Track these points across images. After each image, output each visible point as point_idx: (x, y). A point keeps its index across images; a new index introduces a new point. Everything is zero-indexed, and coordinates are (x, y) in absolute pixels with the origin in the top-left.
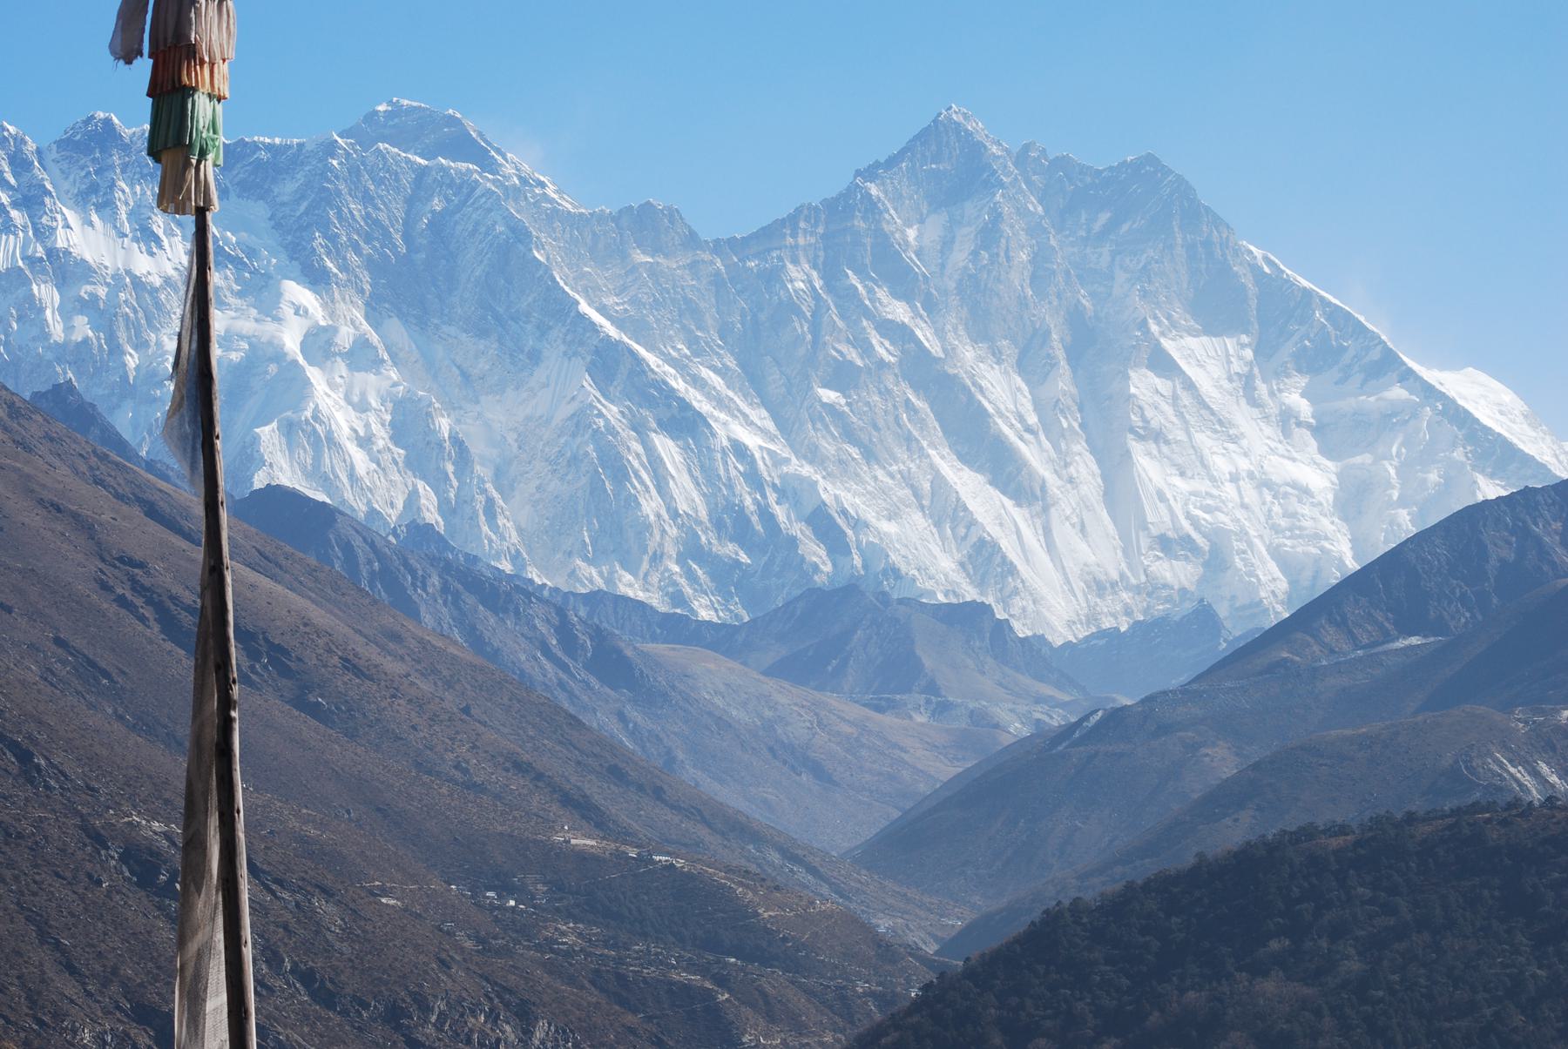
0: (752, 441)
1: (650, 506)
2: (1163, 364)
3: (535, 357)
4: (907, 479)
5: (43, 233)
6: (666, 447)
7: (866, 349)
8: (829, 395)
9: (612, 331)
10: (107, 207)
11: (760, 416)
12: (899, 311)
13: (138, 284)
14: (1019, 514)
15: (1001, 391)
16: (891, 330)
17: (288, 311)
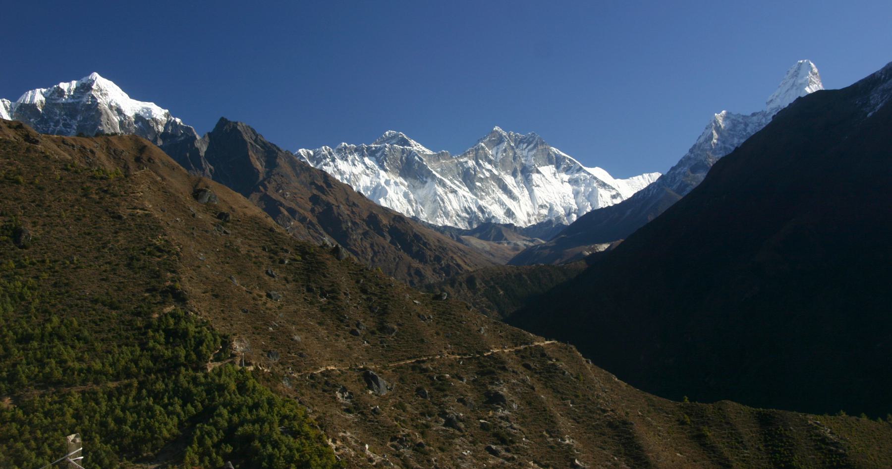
0: (466, 194)
1: (449, 208)
2: (538, 172)
3: (426, 182)
4: (493, 198)
5: (336, 166)
6: (451, 196)
7: (484, 174)
8: (478, 184)
9: (438, 176)
10: (346, 160)
11: (467, 189)
12: (489, 167)
13: (354, 175)
14: (514, 203)
15: (509, 180)
16: (488, 170)
17: (381, 177)
